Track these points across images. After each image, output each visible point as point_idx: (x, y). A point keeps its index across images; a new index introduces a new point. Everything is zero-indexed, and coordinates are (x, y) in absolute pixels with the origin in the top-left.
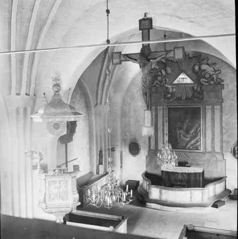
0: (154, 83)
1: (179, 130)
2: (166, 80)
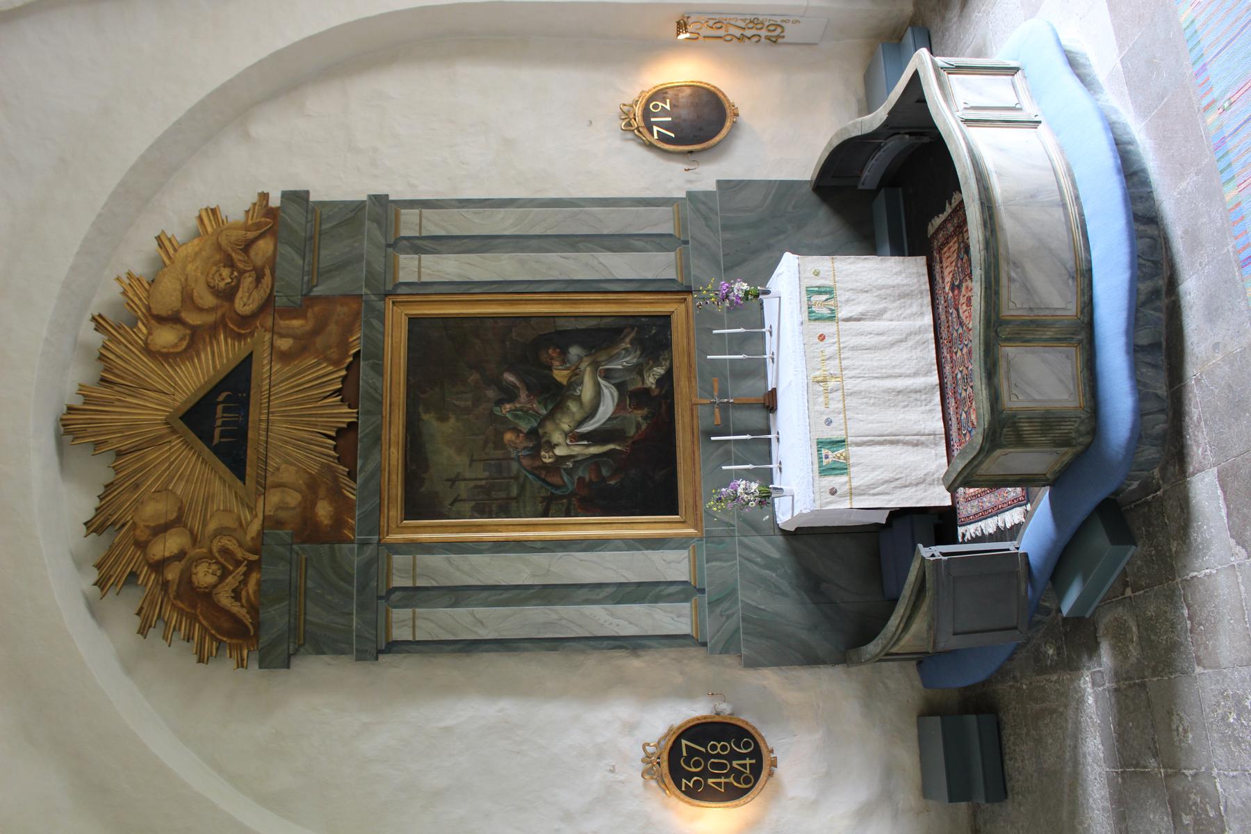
1: (552, 446)
2: (221, 532)
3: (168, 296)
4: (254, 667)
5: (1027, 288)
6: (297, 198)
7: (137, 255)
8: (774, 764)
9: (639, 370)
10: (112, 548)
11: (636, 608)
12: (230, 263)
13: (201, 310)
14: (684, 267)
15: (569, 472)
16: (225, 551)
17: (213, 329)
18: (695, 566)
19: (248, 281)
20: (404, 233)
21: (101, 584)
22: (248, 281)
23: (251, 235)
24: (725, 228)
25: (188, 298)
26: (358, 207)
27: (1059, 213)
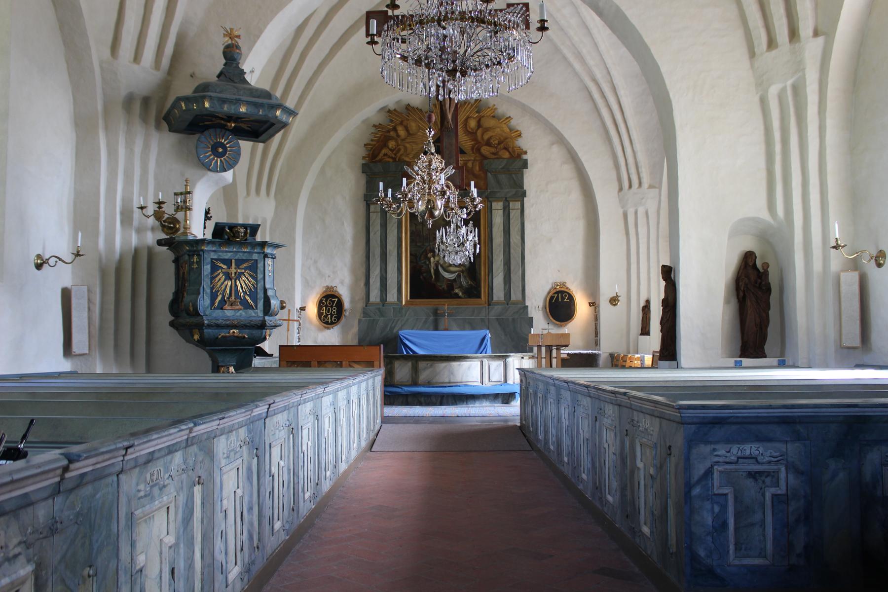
0: (380, 157)
2: (406, 148)
3: (488, 123)
4: (364, 162)
5: (425, 368)
6: (525, 165)
7: (503, 109)
8: (328, 328)
9: (461, 287)
10: (401, 113)
11: (379, 284)
12: (500, 143)
13: (483, 135)
14: (498, 303)
15: (425, 263)
16: (399, 150)
17: (475, 139)
18: (392, 304)
19: (493, 150)
20: (511, 204)
21: (389, 111)
22: (493, 150)
23: (510, 150)
24: (513, 319)
25: (487, 130)
26: (521, 185)
27: (447, 380)
